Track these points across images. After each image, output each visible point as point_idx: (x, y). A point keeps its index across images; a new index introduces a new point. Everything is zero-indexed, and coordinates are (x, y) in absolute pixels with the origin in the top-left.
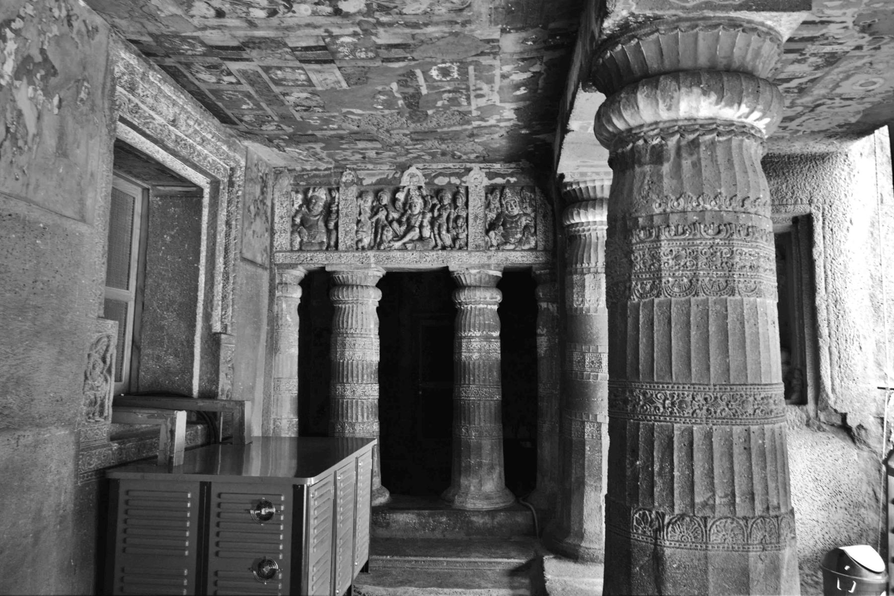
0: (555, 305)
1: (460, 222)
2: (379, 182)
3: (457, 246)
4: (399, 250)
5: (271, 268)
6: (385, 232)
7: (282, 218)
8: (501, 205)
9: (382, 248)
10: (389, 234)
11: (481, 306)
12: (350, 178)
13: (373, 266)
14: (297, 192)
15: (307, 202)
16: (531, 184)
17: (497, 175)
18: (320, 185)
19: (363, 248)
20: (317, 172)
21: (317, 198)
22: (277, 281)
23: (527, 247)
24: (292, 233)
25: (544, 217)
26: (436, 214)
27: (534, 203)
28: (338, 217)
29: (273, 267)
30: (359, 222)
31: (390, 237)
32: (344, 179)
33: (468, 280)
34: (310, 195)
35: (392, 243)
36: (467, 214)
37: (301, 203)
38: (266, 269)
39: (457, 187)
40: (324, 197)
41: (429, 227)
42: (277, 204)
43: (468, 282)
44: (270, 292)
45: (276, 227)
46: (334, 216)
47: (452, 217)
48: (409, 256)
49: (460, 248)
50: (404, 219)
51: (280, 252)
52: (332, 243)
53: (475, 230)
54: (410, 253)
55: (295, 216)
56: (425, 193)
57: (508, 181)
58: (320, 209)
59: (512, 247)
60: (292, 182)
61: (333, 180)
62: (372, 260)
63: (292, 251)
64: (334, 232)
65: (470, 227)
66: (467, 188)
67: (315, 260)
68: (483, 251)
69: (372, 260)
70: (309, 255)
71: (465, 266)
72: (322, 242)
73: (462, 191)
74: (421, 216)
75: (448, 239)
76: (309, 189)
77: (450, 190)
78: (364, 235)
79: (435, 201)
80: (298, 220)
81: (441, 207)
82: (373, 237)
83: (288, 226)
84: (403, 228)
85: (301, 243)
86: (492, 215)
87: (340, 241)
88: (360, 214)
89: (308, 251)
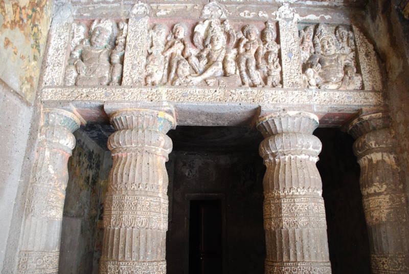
0: (392, 156)
1: (273, 57)
2: (175, 14)
3: (269, 83)
4: (198, 86)
5: (35, 106)
6: (181, 66)
7: (57, 50)
8: (314, 45)
9: (177, 83)
10: (185, 69)
11: (303, 157)
12: (142, 10)
13: (165, 104)
14: (79, 24)
15: (90, 35)
16: (348, 23)
17: (310, 12)
18: (107, 17)
19: (153, 84)
20: (105, 5)
21: (102, 30)
22: (42, 123)
23: (351, 87)
24: (67, 67)
25: (367, 55)
26: (242, 50)
27: (352, 42)
28: (124, 49)
29: (38, 104)
30: (150, 54)
31: (187, 73)
32: (135, 11)
33: (283, 125)
34: (93, 27)
35: (190, 78)
36: (280, 50)
37: (83, 37)
38: (28, 104)
39: (266, 23)
40: (110, 29)
41: (234, 64)
42: (54, 35)
43: (284, 127)
44: (31, 134)
45: (49, 60)
46: (119, 48)
47: (262, 53)
48: (210, 93)
49: (274, 86)
50: (204, 54)
51: (49, 87)
52: (116, 79)
53: (291, 67)
54: (213, 90)
55: (74, 50)
56: (228, 26)
57: (323, 18)
58: (105, 44)
59: (334, 87)
60: (74, 14)
61: (122, 11)
62: (164, 97)
63: (64, 86)
64: (119, 66)
65: (283, 63)
66: (277, 24)
67: (91, 97)
68: (301, 89)
69: (164, 97)
70: (84, 90)
71: (281, 107)
72: (103, 78)
73: (272, 26)
74: (224, 51)
75: (257, 77)
76: (93, 21)
77: (258, 26)
78: (155, 69)
79: (241, 35)
80: (77, 54)
81: (247, 42)
82: (166, 72)
83: (63, 59)
84: (204, 62)
85: (76, 79)
86: (306, 55)
87: (124, 75)
88: (152, 46)
89: (84, 87)
